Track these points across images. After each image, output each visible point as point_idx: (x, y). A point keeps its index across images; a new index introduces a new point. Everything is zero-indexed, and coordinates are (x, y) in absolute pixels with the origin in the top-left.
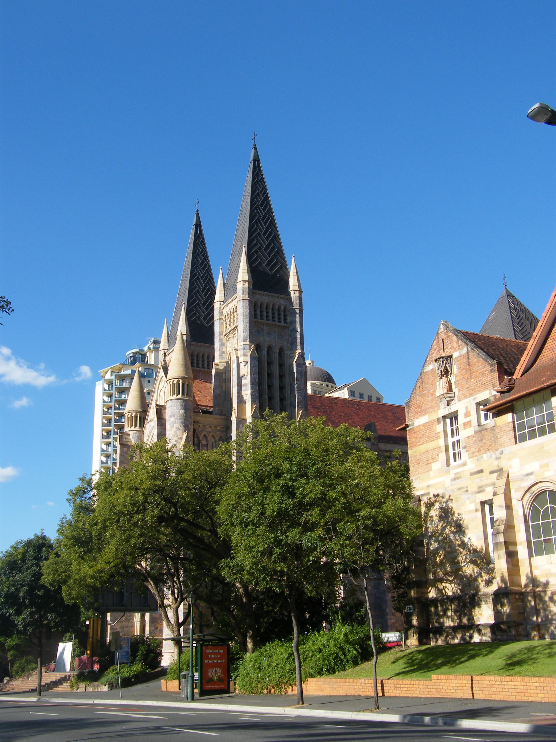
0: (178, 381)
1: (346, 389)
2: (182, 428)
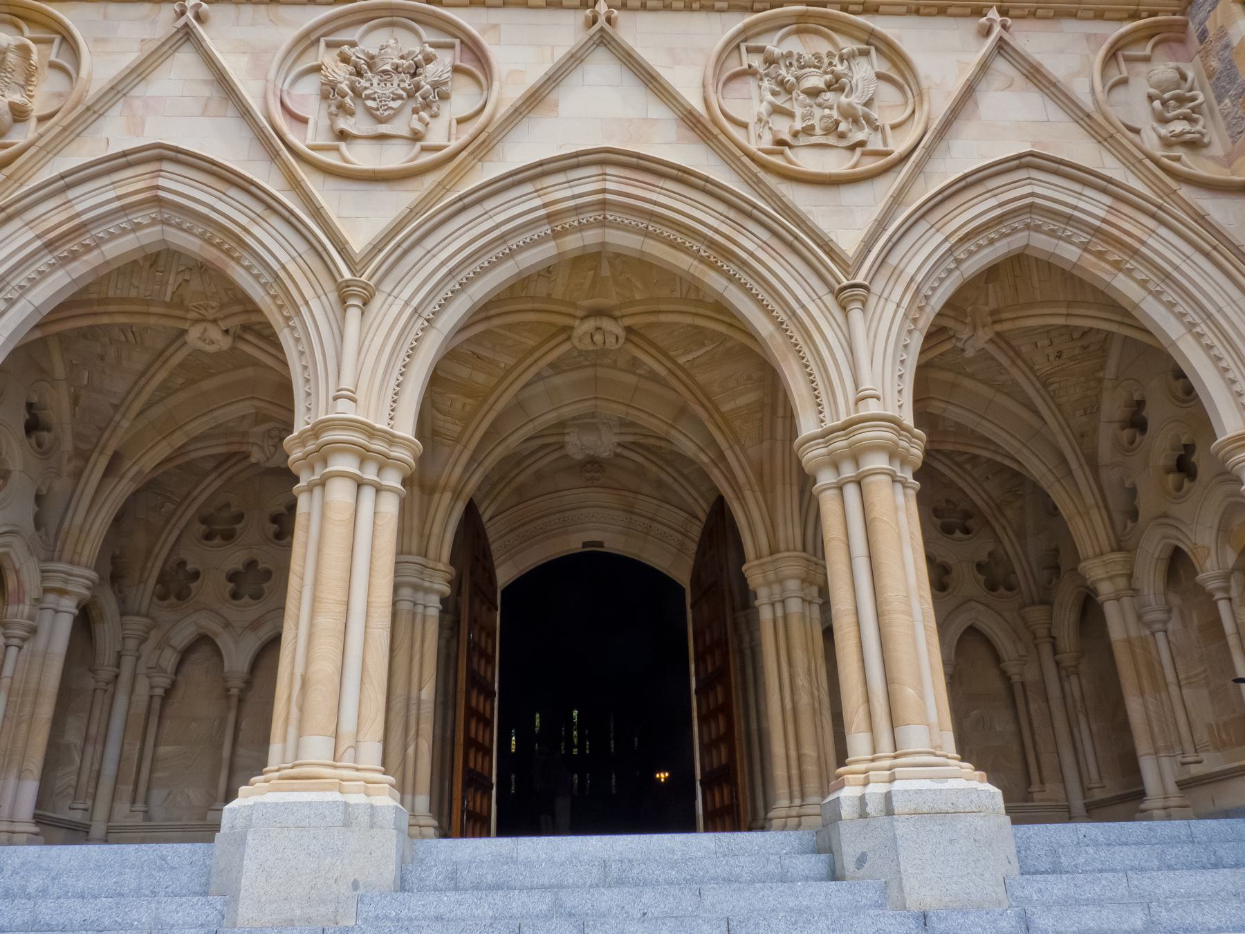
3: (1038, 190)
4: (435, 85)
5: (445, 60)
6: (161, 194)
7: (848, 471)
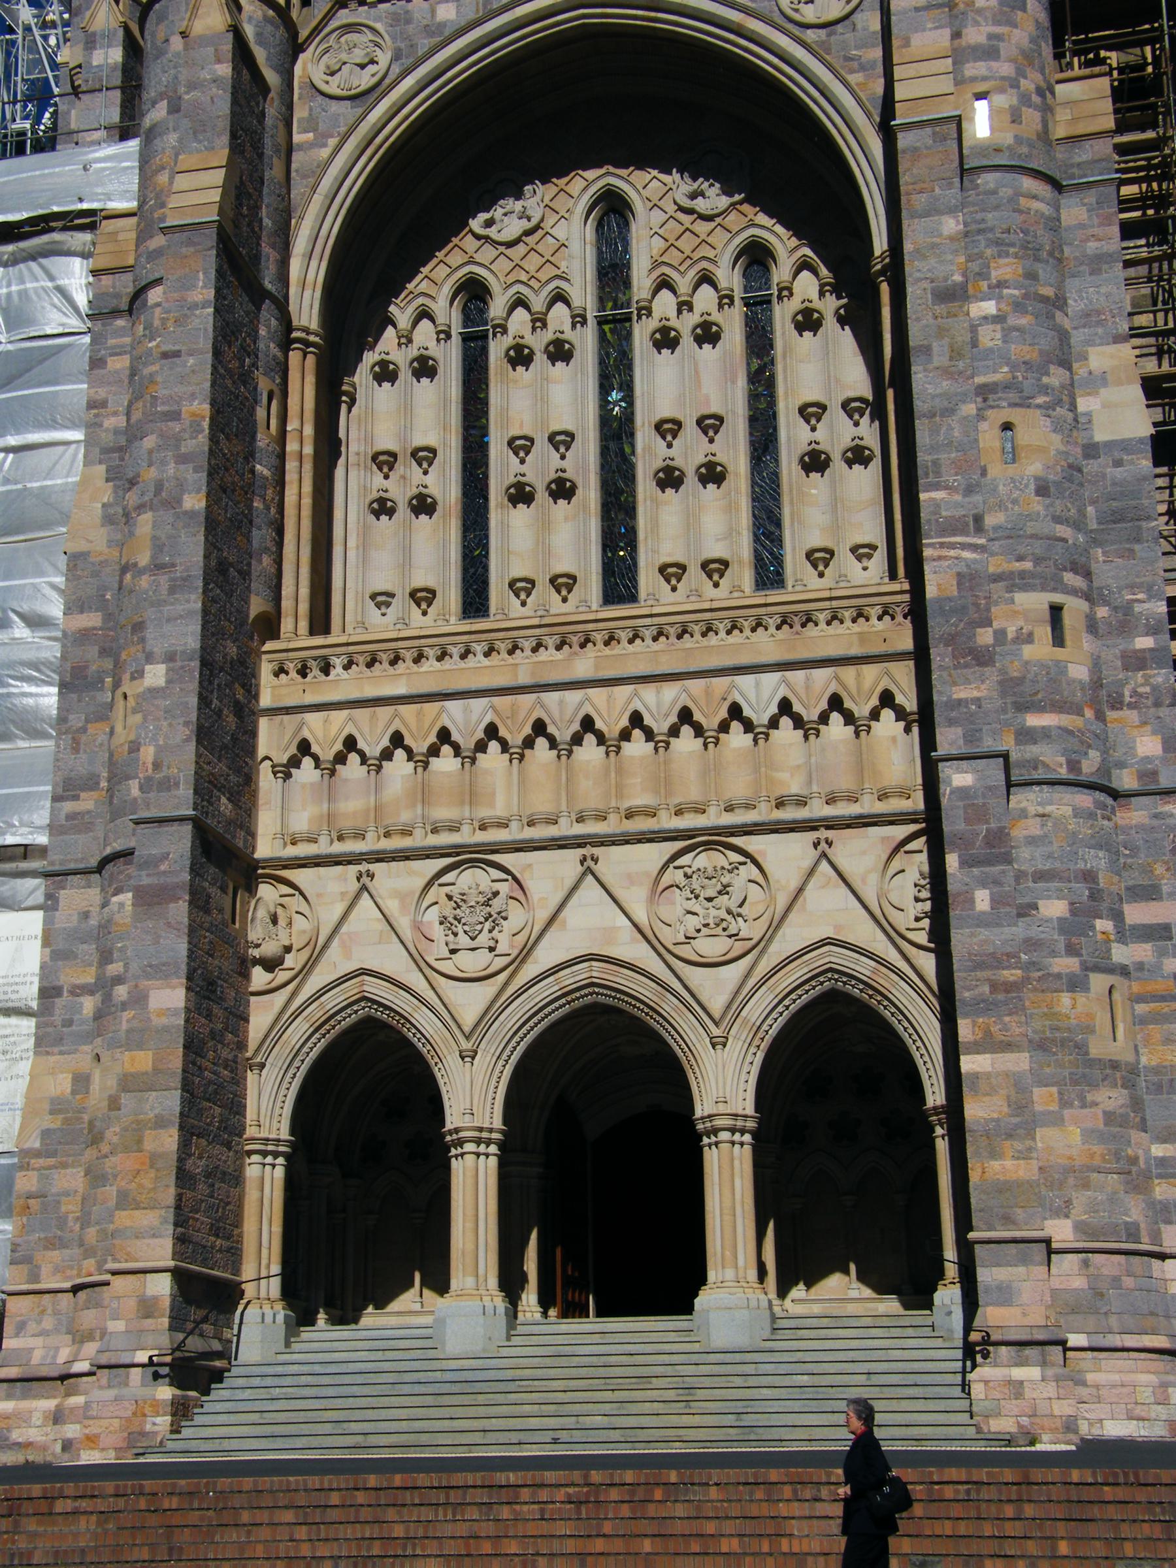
3: (833, 960)
4: (499, 913)
5: (504, 888)
6: (367, 994)
7: (713, 1139)
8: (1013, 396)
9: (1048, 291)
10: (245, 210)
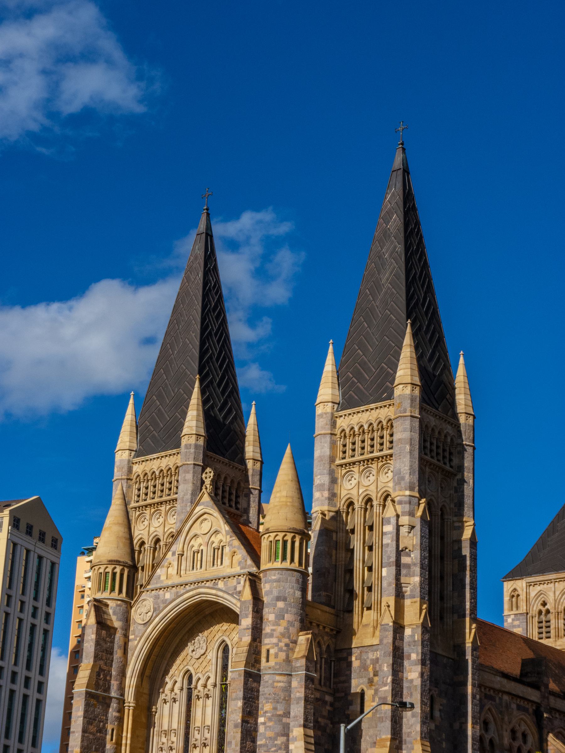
0: (294, 537)
1: (7, 512)
2: (297, 624)
8: (265, 749)
9: (280, 712)
10: (102, 676)
